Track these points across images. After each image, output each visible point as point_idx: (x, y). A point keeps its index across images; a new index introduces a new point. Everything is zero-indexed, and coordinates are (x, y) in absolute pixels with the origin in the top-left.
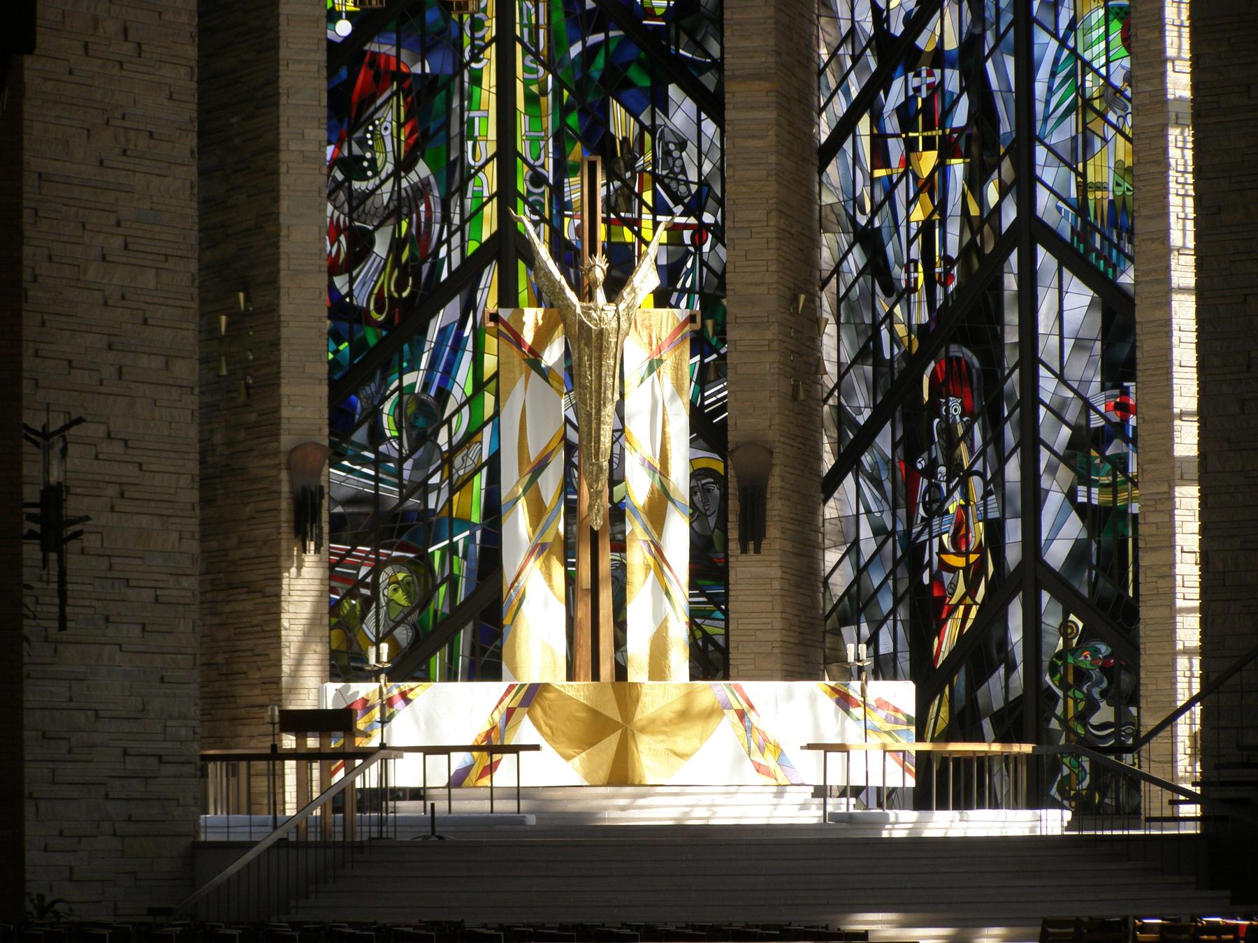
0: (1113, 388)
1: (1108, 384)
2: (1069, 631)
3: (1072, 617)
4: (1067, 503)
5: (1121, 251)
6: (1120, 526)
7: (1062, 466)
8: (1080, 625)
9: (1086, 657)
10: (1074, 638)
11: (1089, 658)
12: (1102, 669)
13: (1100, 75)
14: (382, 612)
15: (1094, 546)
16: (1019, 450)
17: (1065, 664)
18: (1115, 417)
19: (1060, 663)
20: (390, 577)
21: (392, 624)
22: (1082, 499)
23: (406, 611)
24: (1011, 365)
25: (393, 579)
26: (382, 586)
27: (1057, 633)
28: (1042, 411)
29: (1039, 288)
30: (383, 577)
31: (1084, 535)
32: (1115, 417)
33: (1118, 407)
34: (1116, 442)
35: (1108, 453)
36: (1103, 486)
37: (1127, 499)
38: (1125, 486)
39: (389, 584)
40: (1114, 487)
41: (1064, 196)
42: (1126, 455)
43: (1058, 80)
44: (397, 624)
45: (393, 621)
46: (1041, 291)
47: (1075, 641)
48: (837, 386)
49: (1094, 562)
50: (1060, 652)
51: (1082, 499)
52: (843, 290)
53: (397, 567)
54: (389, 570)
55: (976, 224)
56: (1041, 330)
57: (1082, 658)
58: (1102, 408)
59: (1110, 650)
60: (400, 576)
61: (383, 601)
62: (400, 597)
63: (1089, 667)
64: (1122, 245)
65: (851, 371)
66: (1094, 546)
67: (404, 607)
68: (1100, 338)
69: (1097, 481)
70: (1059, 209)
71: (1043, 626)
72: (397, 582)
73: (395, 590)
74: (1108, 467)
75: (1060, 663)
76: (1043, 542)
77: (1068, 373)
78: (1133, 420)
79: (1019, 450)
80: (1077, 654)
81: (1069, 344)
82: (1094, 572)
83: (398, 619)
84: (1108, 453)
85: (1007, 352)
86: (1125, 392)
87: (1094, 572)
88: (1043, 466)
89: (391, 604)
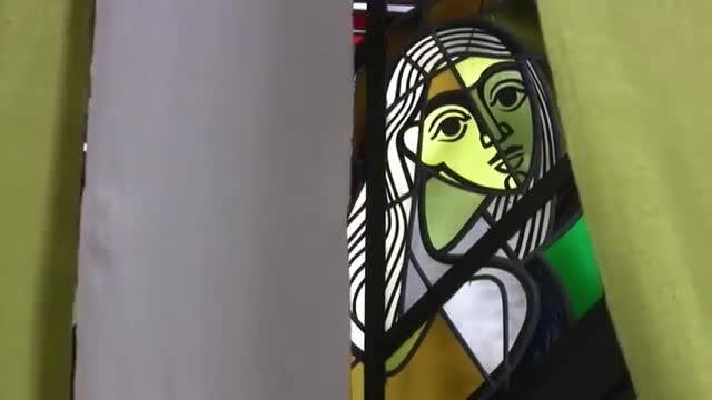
14: (396, 222)
20: (426, 80)
21: (436, 272)
23: (497, 210)
25: (440, 85)
26: (395, 117)
30: (400, 80)
39: (425, 107)
44: (461, 271)
45: (439, 255)
53: (455, 40)
54: (426, 52)
60: (471, 71)
61: (399, 178)
62: (474, 159)
67: (490, 193)
72: (460, 95)
73: (451, 128)
83: (461, 249)
89: (432, 186)
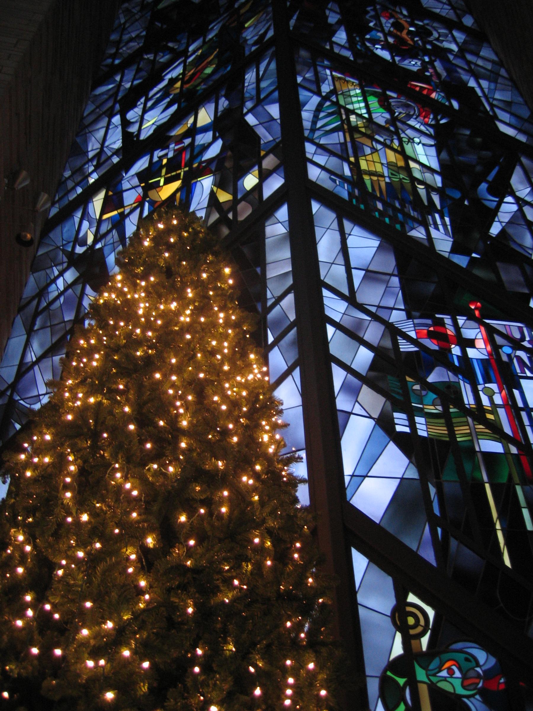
0: (421, 317)
1: (414, 313)
2: (411, 621)
3: (412, 598)
4: (380, 432)
5: (407, 216)
6: (468, 467)
7: (365, 389)
8: (431, 613)
9: (451, 672)
10: (423, 634)
11: (458, 674)
12: (482, 692)
13: (364, 118)
15: (433, 491)
16: (297, 373)
17: (413, 683)
18: (432, 345)
19: (401, 681)
22: (402, 428)
24: (278, 293)
27: (387, 623)
28: (330, 330)
29: (316, 228)
31: (413, 474)
32: (432, 345)
33: (431, 335)
34: (437, 370)
35: (431, 379)
36: (428, 416)
37: (470, 434)
38: (464, 419)
40: (445, 416)
41: (339, 172)
42: (459, 383)
43: (322, 115)
46: (318, 232)
47: (425, 641)
48: (13, 387)
49: (437, 511)
50: (399, 658)
51: (402, 428)
52: (44, 304)
55: (226, 208)
56: (322, 257)
57: (444, 673)
58: (413, 334)
59: (492, 661)
63: (460, 691)
64: (406, 210)
65: (36, 368)
66: (433, 491)
68: (396, 273)
69: (422, 409)
70: (334, 181)
71: (362, 611)
74: (432, 396)
75: (401, 681)
76: (347, 479)
77: (361, 298)
78: (456, 350)
79: (297, 373)
80: (434, 664)
81: (358, 276)
82: (439, 530)
84: (431, 379)
85: (270, 285)
86: (441, 323)
87: (439, 530)
88: (337, 384)
